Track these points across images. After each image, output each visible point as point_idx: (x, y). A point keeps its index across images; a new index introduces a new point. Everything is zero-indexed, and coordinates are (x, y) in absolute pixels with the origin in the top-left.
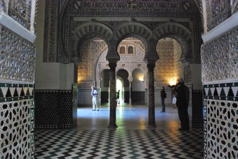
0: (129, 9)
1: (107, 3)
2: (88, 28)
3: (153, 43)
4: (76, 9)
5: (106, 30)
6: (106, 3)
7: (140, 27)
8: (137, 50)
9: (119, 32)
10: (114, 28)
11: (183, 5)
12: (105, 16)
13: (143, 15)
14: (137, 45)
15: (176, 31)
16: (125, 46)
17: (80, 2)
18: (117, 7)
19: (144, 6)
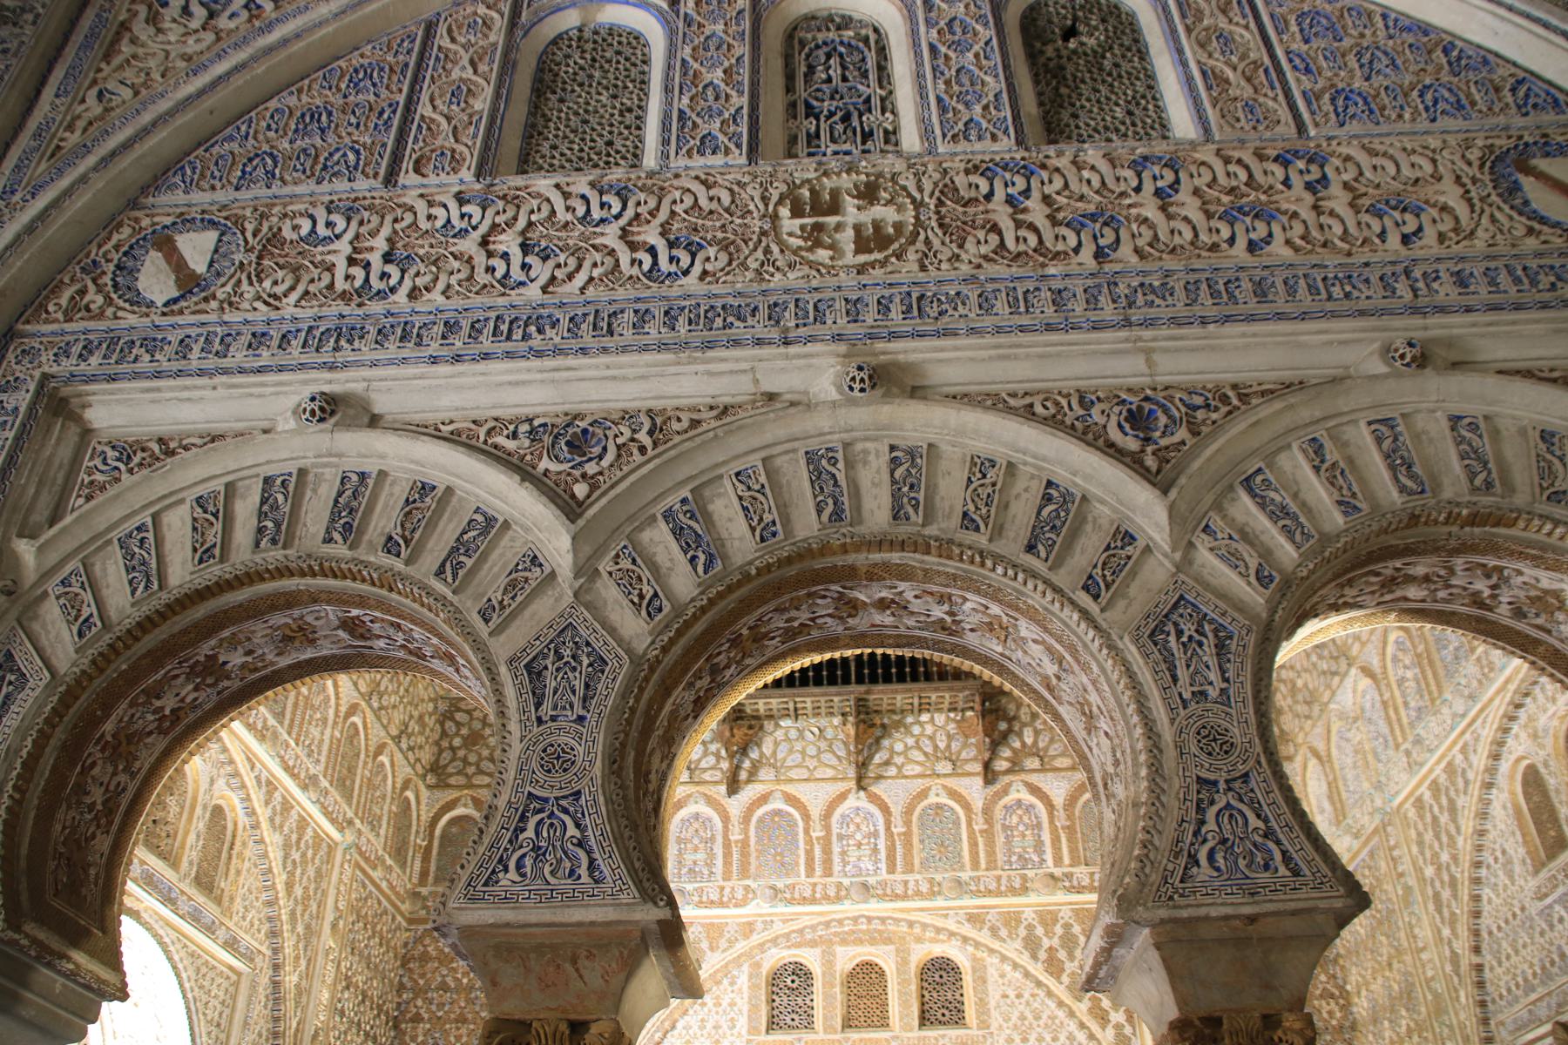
0: (811, 264)
1: (530, 224)
2: (246, 510)
3: (1208, 653)
4: (151, 304)
5: (488, 525)
6: (521, 223)
7: (981, 466)
8: (994, 998)
9: (678, 532)
10: (594, 487)
11: (1515, 188)
12: (486, 356)
13: (1001, 306)
14: (996, 945)
15: (1523, 475)
16: (885, 957)
17: (212, 236)
18: (652, 251)
19: (1007, 225)
